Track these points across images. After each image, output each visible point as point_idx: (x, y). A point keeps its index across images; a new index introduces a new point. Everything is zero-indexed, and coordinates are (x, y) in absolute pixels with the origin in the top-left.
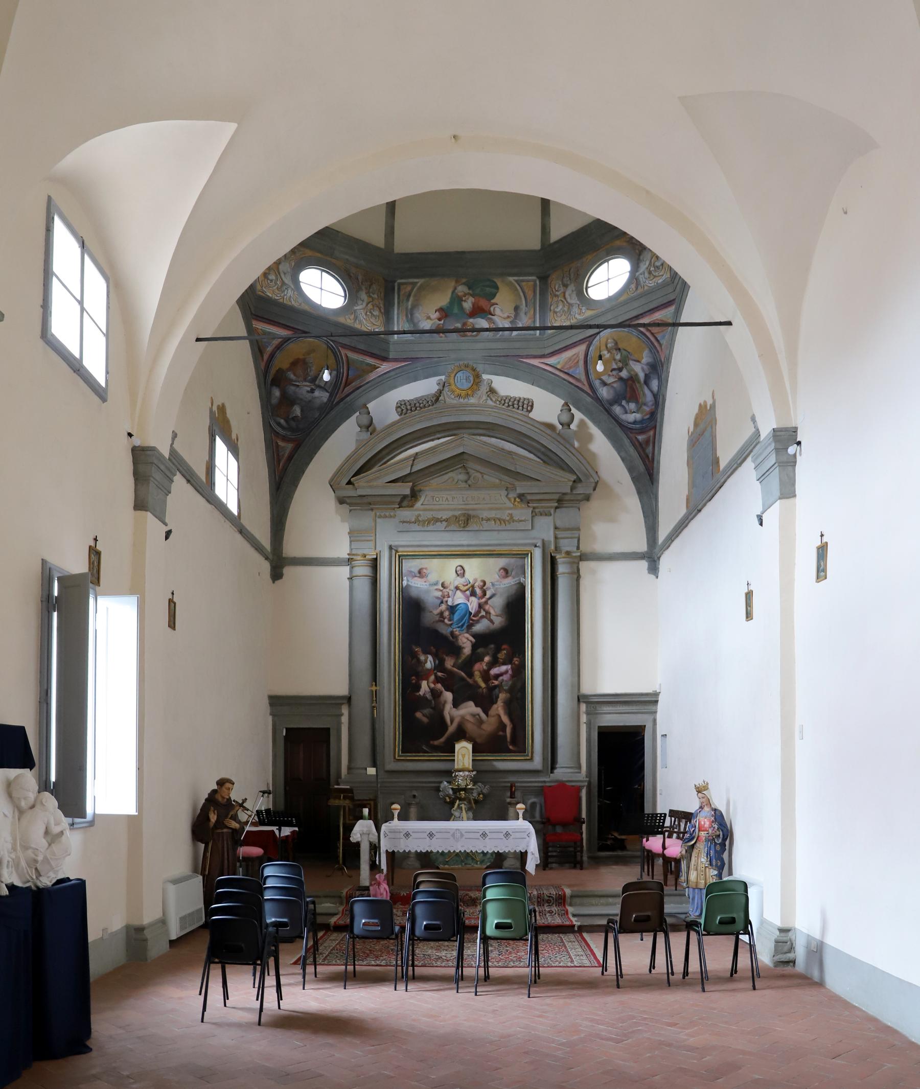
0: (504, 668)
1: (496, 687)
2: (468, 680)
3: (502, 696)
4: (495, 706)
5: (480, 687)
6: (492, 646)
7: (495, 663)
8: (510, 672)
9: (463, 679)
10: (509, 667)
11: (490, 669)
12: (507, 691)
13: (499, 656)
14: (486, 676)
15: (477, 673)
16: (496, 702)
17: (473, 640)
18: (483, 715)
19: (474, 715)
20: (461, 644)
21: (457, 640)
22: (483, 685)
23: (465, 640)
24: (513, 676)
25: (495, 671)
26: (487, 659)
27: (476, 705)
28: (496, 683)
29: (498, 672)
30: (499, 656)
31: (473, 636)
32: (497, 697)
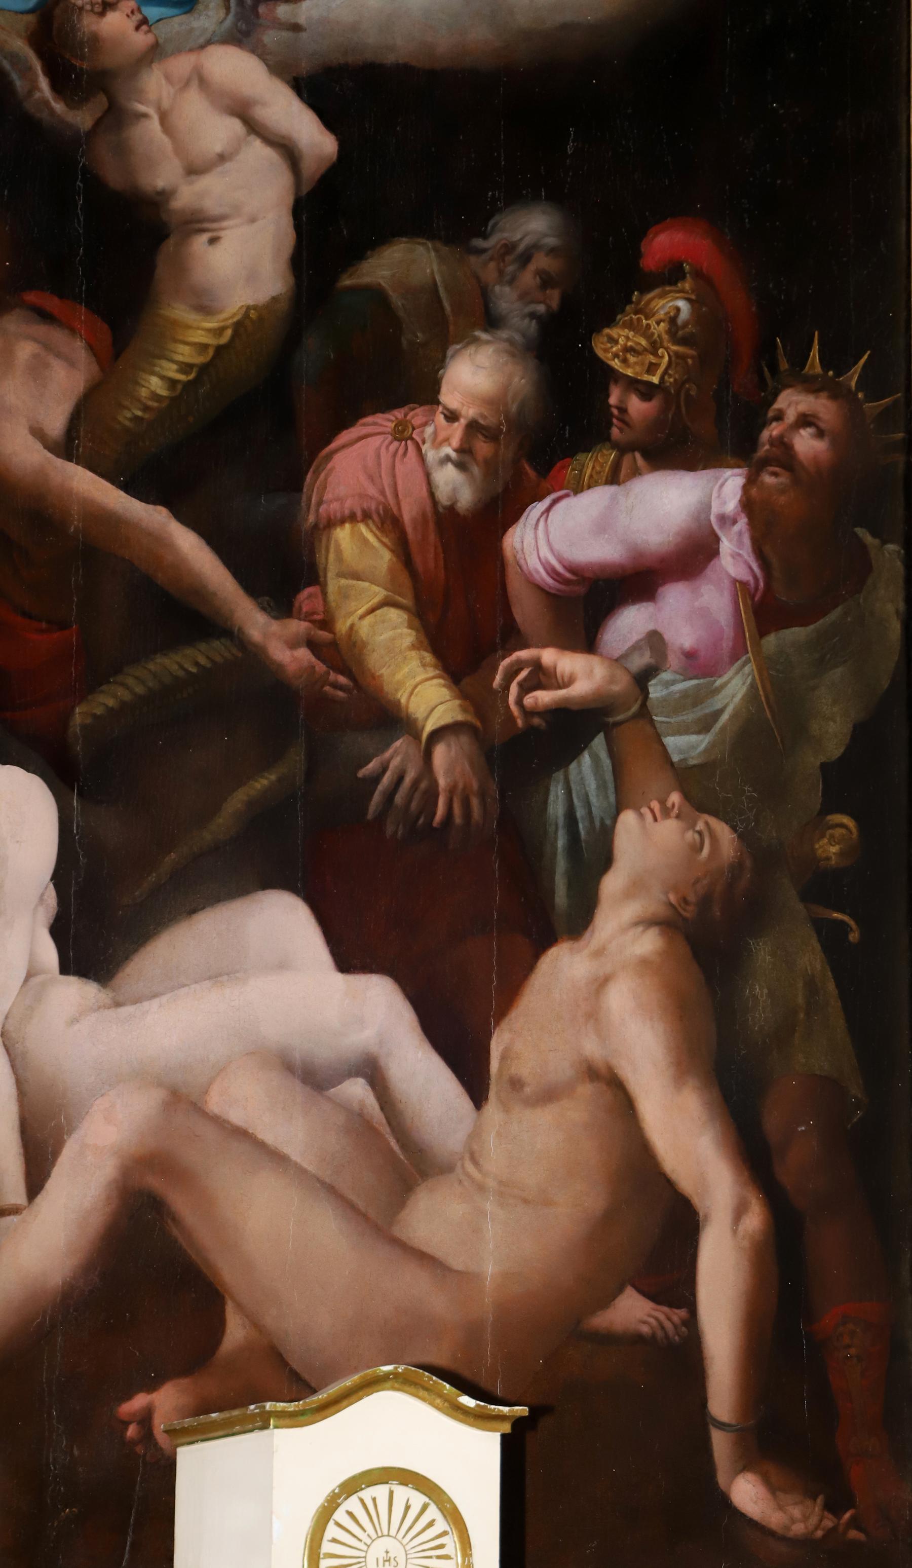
0: (664, 503)
1: (575, 726)
2: (255, 622)
3: (651, 847)
4: (564, 967)
5: (389, 720)
6: (534, 225)
7: (565, 426)
8: (735, 557)
9: (184, 616)
10: (726, 488)
11: (503, 506)
12: (700, 789)
13: (615, 345)
14: (463, 593)
15: (356, 555)
16: (580, 919)
17: (315, 138)
18: (423, 1076)
19: (312, 1077)
20: (163, 174)
21: (116, 117)
22: (428, 697)
23: (216, 131)
24: (764, 610)
25: (560, 534)
26: (474, 376)
27: (349, 957)
28: (581, 675)
29: (601, 551)
30: (615, 345)
31: (319, 88)
32: (593, 856)
